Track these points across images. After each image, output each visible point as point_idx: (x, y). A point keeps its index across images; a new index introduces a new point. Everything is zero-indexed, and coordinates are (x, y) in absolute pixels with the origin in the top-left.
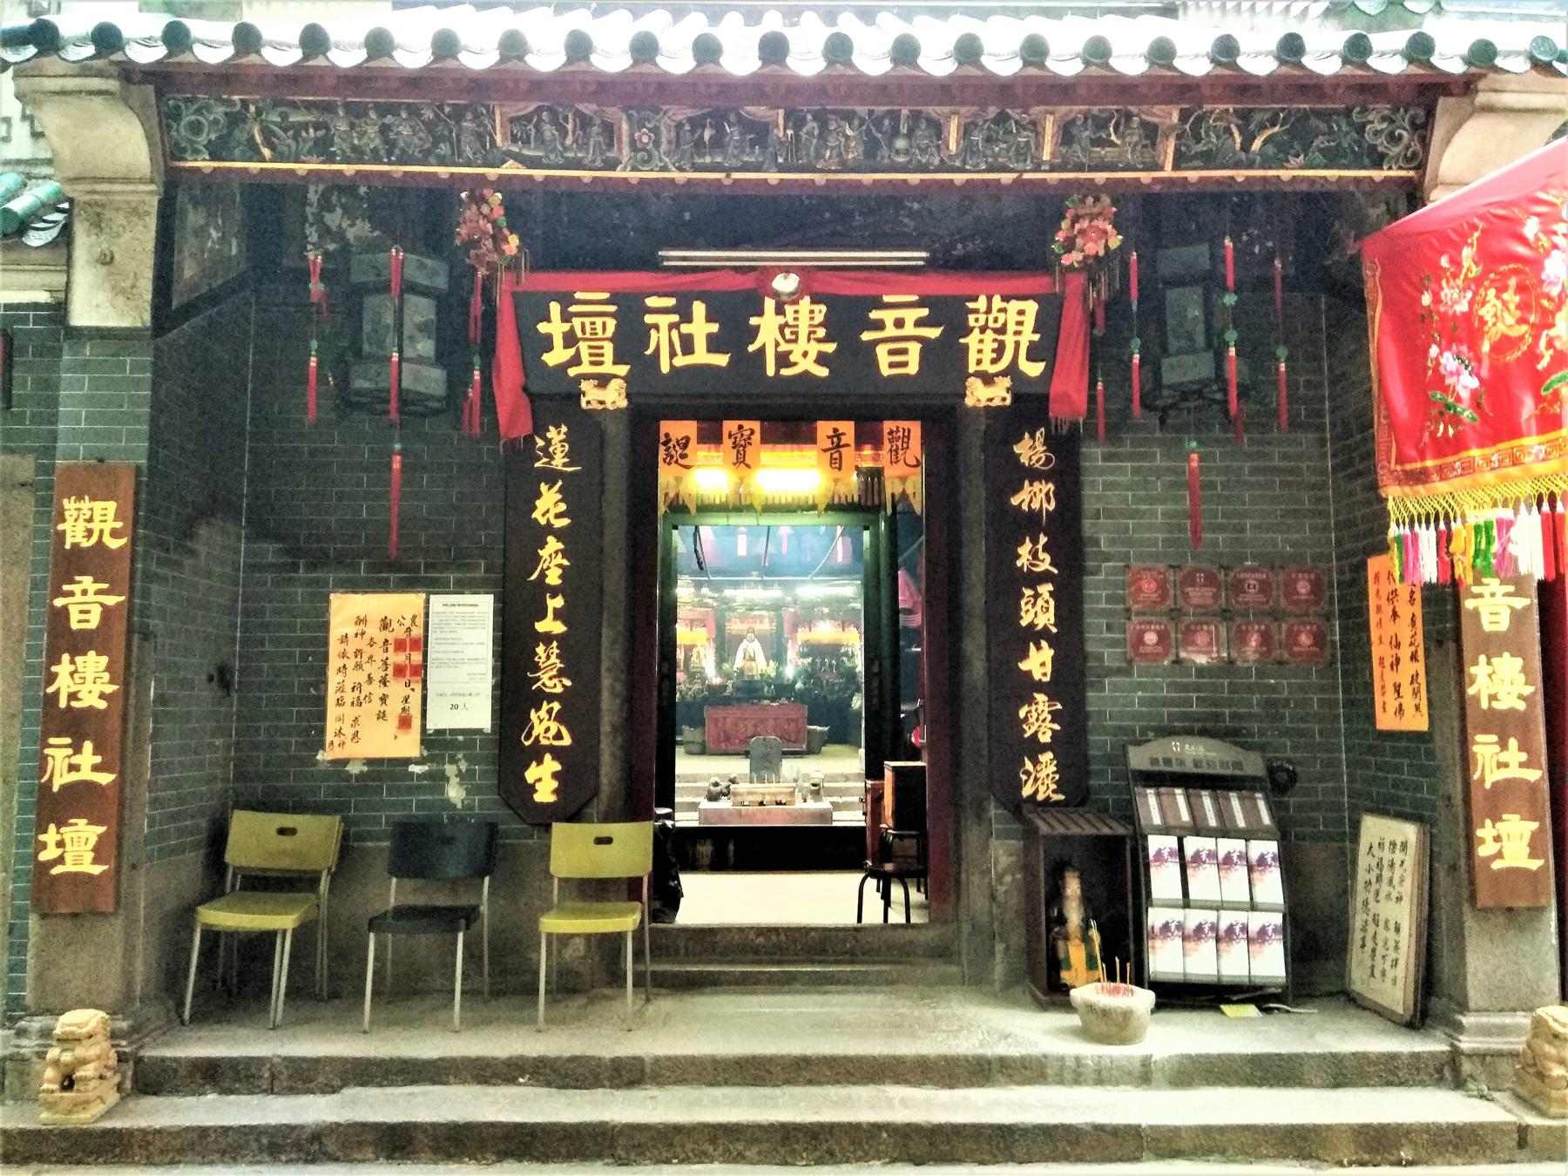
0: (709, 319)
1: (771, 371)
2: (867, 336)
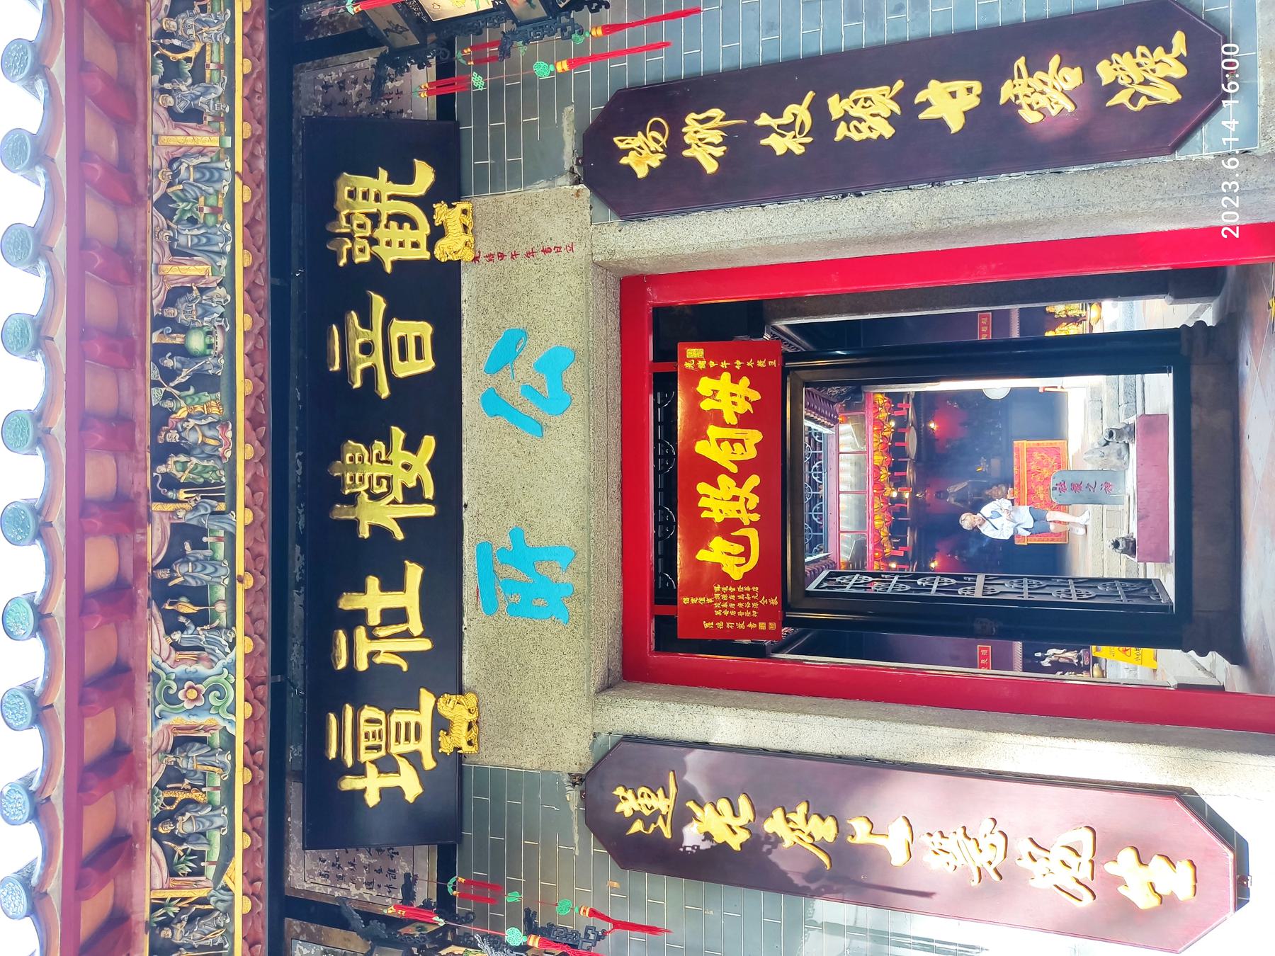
0: (362, 589)
1: (428, 511)
2: (384, 391)
